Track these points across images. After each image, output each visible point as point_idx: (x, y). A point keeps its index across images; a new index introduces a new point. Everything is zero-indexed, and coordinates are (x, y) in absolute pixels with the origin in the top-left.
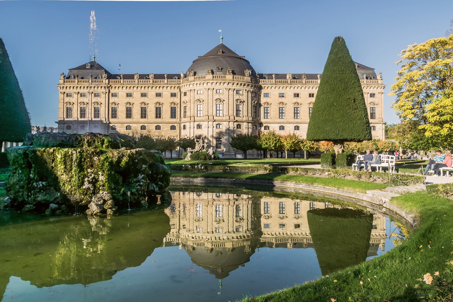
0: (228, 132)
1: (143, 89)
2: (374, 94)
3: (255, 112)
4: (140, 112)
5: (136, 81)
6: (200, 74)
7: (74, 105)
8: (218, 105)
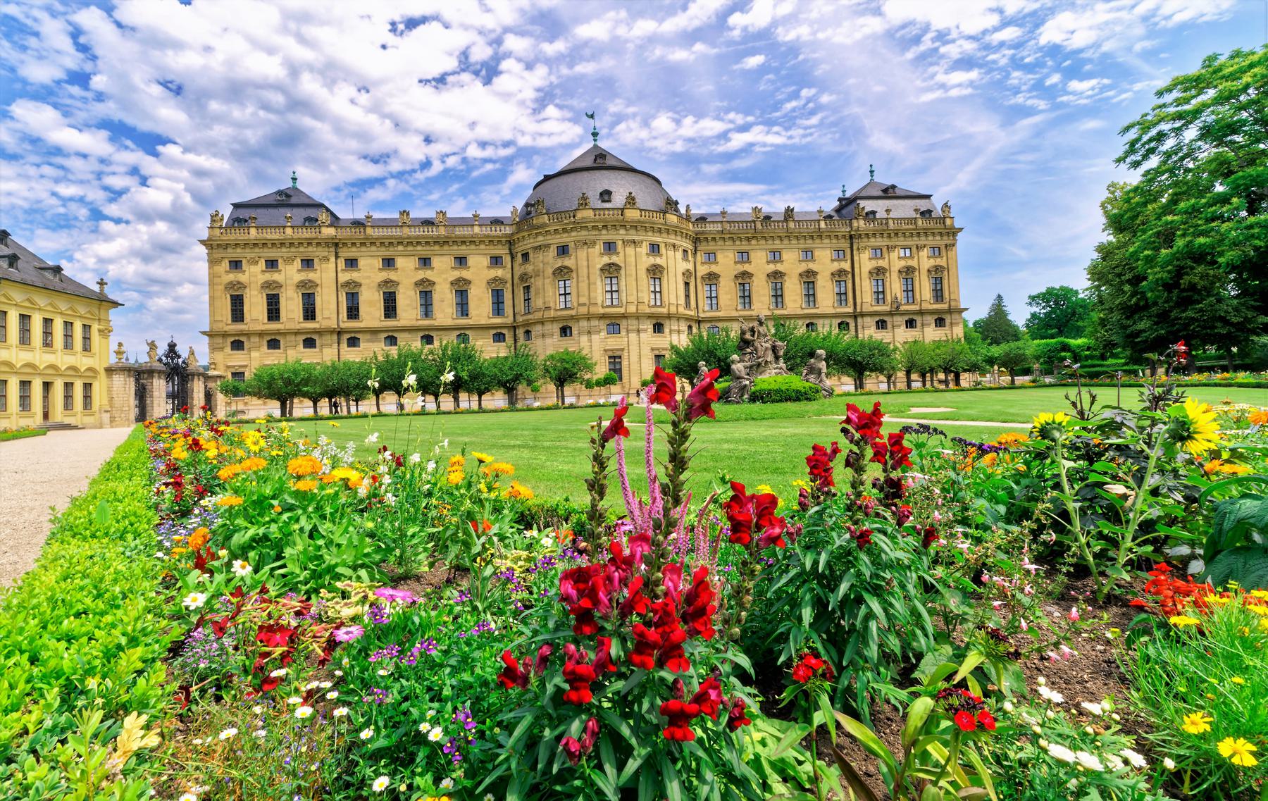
7: (247, 290)
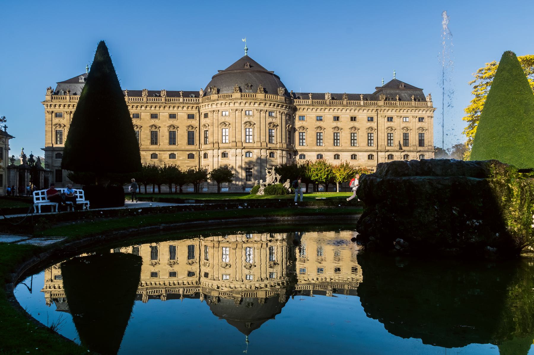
0: (259, 161)
1: (153, 108)
2: (423, 118)
3: (289, 138)
4: (149, 137)
5: (145, 99)
6: (225, 92)
8: (248, 129)
